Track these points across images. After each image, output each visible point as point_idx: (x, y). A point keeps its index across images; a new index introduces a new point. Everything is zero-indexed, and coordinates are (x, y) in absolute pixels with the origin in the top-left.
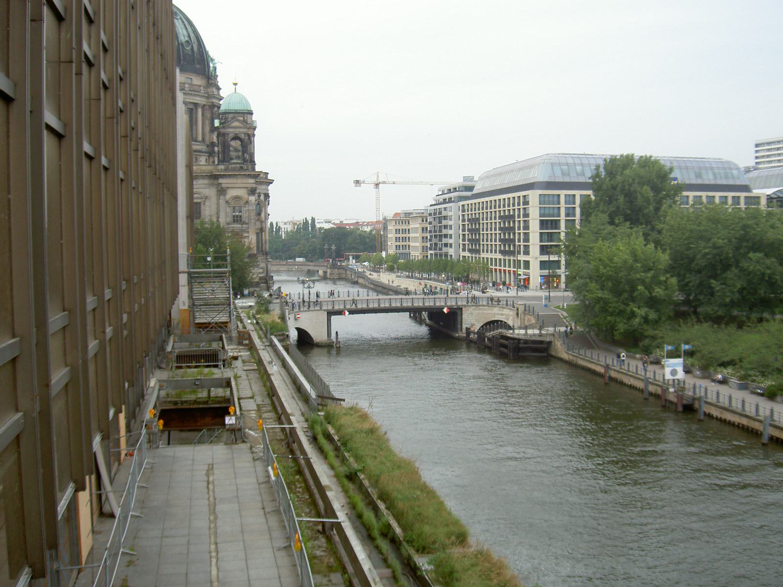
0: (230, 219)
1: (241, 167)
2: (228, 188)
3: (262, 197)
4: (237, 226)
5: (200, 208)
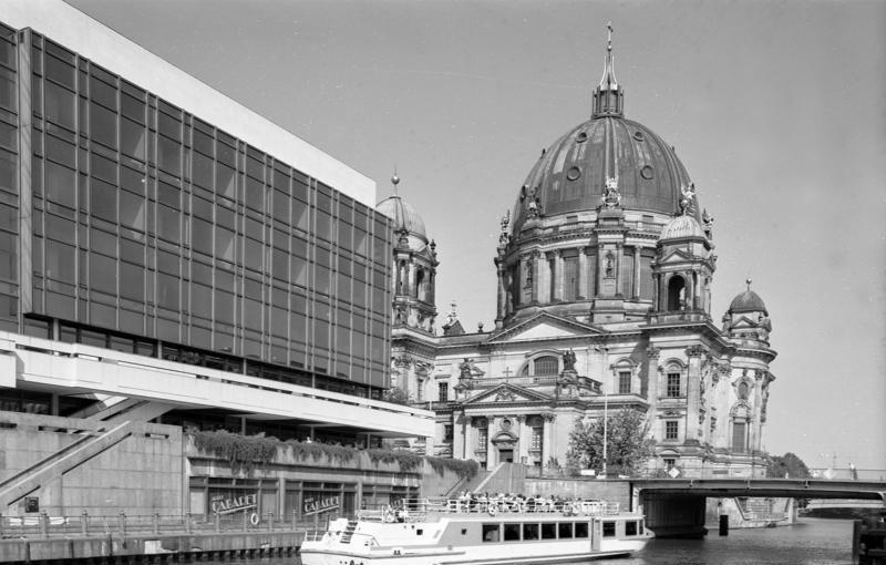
0: (662, 391)
1: (681, 319)
2: (661, 348)
3: (751, 374)
5: (630, 379)
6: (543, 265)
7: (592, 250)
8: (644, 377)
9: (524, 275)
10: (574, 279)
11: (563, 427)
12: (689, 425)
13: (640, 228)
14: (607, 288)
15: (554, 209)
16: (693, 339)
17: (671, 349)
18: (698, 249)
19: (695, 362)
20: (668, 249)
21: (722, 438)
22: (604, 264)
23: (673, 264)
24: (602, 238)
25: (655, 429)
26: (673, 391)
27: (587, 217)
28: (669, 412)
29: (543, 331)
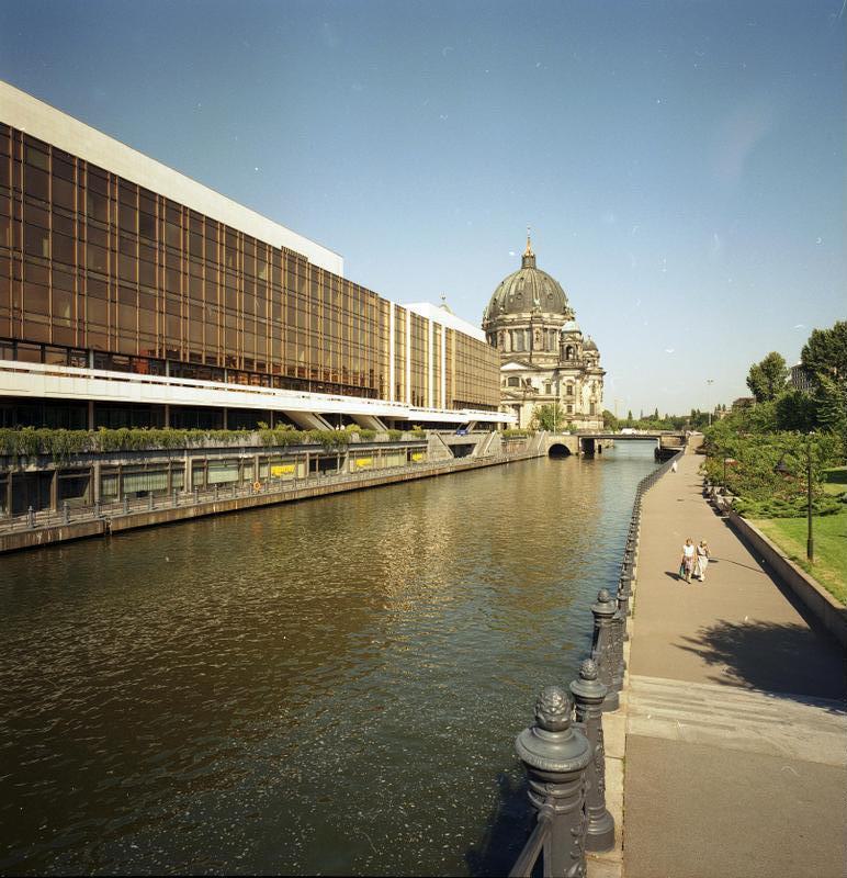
0: (565, 393)
4: (569, 397)
6: (507, 335)
7: (530, 330)
8: (557, 386)
9: (499, 339)
10: (521, 341)
11: (528, 409)
12: (576, 407)
13: (549, 321)
14: (537, 346)
15: (511, 311)
16: (577, 372)
17: (569, 376)
18: (577, 335)
19: (578, 381)
20: (566, 335)
21: (586, 411)
22: (535, 336)
23: (568, 341)
24: (534, 325)
25: (563, 407)
26: (570, 393)
27: (527, 316)
28: (568, 402)
29: (513, 366)
